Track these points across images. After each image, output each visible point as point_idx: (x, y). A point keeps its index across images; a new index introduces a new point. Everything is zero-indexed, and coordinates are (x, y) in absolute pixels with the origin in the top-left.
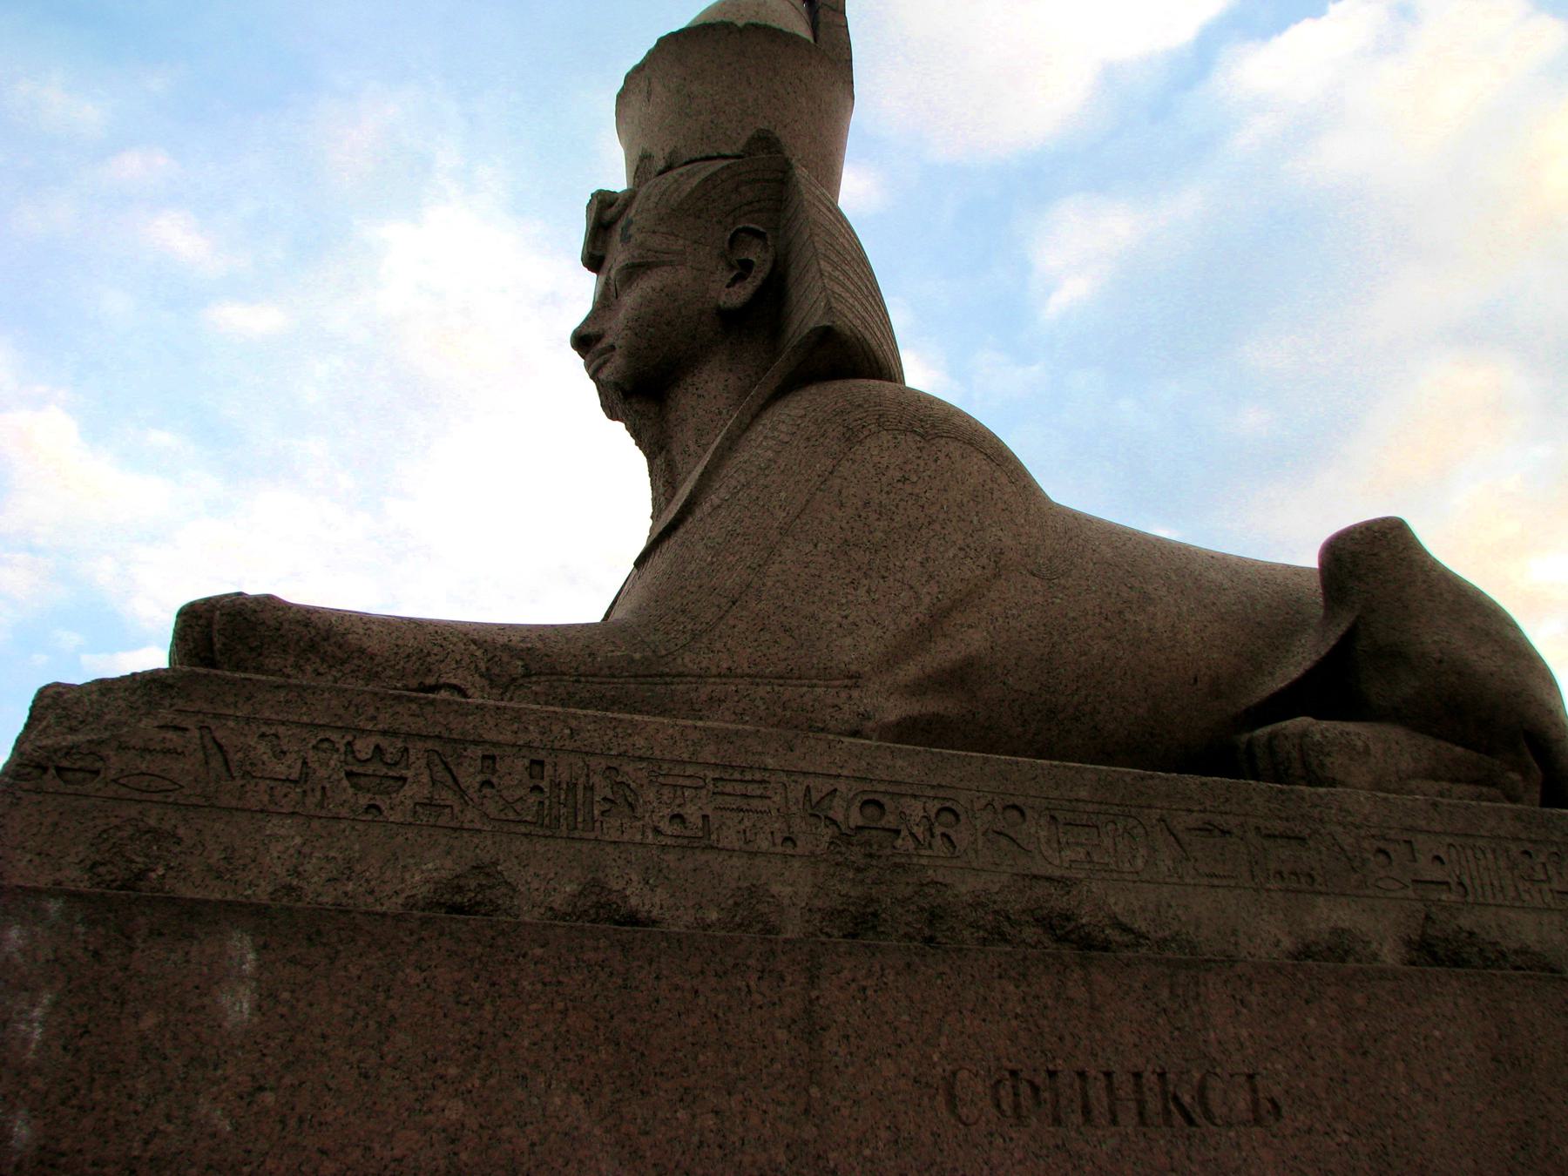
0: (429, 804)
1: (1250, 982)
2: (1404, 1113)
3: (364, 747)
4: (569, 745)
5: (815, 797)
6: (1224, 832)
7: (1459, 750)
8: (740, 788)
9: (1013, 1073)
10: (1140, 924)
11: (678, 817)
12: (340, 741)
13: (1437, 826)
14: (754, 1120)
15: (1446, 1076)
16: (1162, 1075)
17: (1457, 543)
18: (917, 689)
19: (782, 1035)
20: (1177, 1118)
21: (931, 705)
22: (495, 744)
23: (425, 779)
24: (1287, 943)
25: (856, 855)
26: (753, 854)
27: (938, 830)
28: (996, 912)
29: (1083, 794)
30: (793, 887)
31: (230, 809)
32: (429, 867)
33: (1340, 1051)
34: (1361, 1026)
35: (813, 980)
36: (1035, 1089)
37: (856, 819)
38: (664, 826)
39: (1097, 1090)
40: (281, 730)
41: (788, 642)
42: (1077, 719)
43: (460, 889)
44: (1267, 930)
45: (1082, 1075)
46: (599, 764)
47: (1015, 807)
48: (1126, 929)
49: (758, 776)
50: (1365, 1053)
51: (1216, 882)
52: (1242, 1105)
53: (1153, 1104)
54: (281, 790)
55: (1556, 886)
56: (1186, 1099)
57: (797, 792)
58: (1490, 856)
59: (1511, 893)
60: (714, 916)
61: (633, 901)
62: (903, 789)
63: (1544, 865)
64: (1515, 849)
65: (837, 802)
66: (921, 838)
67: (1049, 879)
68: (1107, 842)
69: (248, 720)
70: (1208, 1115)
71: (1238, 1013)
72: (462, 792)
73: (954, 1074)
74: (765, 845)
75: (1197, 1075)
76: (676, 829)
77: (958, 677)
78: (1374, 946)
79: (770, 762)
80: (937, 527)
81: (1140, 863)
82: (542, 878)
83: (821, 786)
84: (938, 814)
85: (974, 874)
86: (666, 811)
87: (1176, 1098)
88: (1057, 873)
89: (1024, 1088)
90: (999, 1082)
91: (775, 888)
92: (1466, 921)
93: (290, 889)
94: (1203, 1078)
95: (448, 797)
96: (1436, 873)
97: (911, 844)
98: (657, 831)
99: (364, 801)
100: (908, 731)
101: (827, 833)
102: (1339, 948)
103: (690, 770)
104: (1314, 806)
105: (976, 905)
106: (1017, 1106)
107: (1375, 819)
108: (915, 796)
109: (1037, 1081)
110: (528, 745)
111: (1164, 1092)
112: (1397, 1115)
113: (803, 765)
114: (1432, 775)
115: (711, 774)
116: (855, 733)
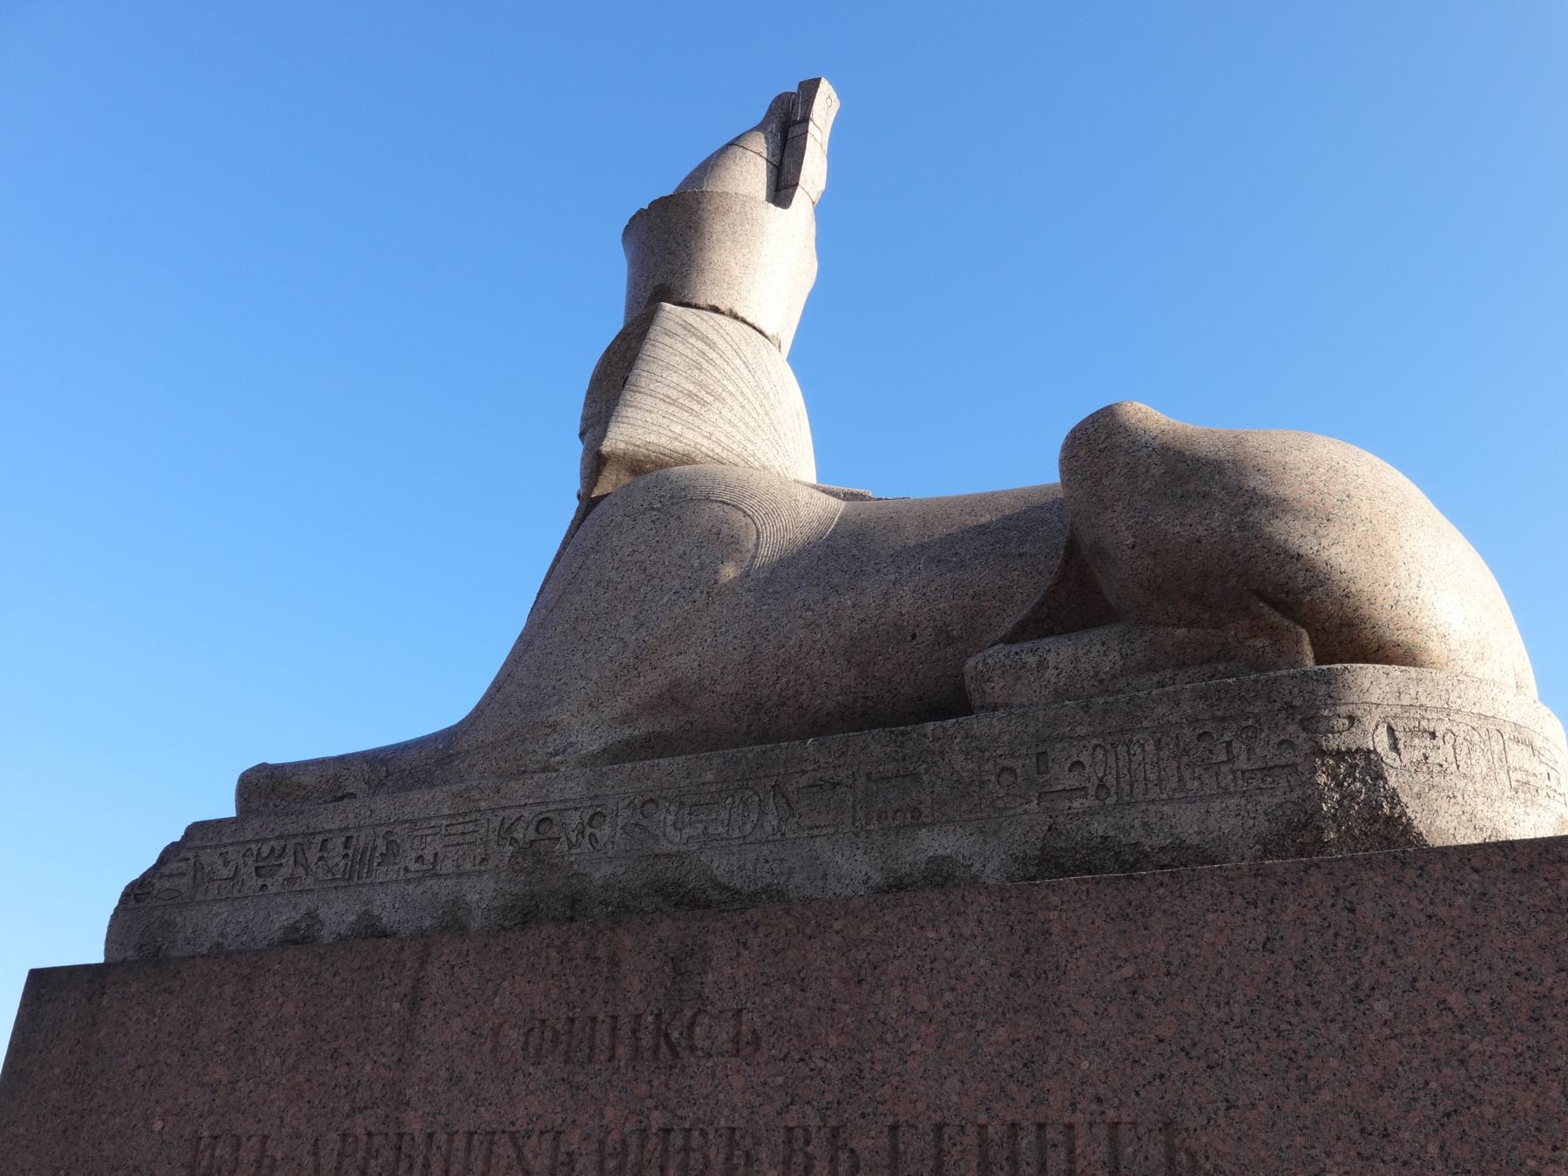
0: (291, 879)
1: (756, 927)
2: (889, 1037)
3: (265, 851)
4: (368, 821)
5: (507, 824)
6: (834, 785)
7: (1181, 632)
8: (460, 827)
9: (543, 1021)
10: (737, 882)
11: (420, 858)
12: (253, 846)
13: (1081, 730)
14: (368, 1068)
15: (948, 997)
16: (658, 1016)
17: (1152, 414)
18: (627, 719)
19: (396, 1006)
20: (664, 1049)
21: (644, 727)
22: (330, 831)
23: (291, 862)
24: (877, 878)
25: (528, 863)
26: (460, 875)
27: (588, 831)
28: (622, 890)
29: (709, 777)
30: (482, 894)
31: (200, 903)
32: (285, 916)
33: (834, 982)
34: (862, 955)
35: (423, 964)
36: (556, 1033)
37: (532, 835)
38: (413, 866)
39: (603, 1033)
40: (230, 849)
41: (517, 711)
42: (784, 704)
43: (298, 930)
44: (853, 865)
45: (594, 1019)
46: (382, 831)
47: (652, 800)
48: (727, 888)
49: (473, 817)
50: (860, 982)
51: (815, 832)
52: (724, 1037)
53: (646, 1041)
54: (224, 884)
55: (1242, 763)
56: (675, 1035)
57: (496, 824)
58: (1150, 747)
59: (1173, 783)
60: (427, 923)
61: (385, 920)
62: (568, 805)
63: (1229, 744)
64: (1188, 733)
65: (521, 826)
66: (574, 840)
67: (668, 856)
68: (724, 815)
69: (217, 846)
70: (692, 1049)
71: (739, 955)
72: (306, 867)
73: (501, 1025)
74: (468, 866)
75: (689, 1013)
76: (417, 866)
77: (674, 697)
78: (978, 866)
79: (483, 805)
80: (656, 581)
81: (749, 827)
82: (338, 913)
83: (514, 814)
84: (592, 817)
85: (602, 864)
86: (414, 855)
87: (667, 1036)
88: (675, 849)
89: (548, 1035)
90: (531, 1029)
91: (468, 899)
92: (1098, 827)
93: (219, 944)
94: (695, 1015)
95: (301, 871)
96: (1071, 780)
97: (565, 847)
98: (407, 870)
99: (260, 883)
100: (620, 753)
101: (509, 849)
102: (941, 875)
103: (433, 823)
104: (936, 739)
105: (606, 887)
106: (538, 1050)
107: (1006, 738)
108: (576, 809)
109: (558, 1027)
110: (347, 829)
111: (658, 1030)
112: (881, 1040)
113: (504, 802)
114: (1150, 667)
115: (444, 822)
116: (544, 770)
